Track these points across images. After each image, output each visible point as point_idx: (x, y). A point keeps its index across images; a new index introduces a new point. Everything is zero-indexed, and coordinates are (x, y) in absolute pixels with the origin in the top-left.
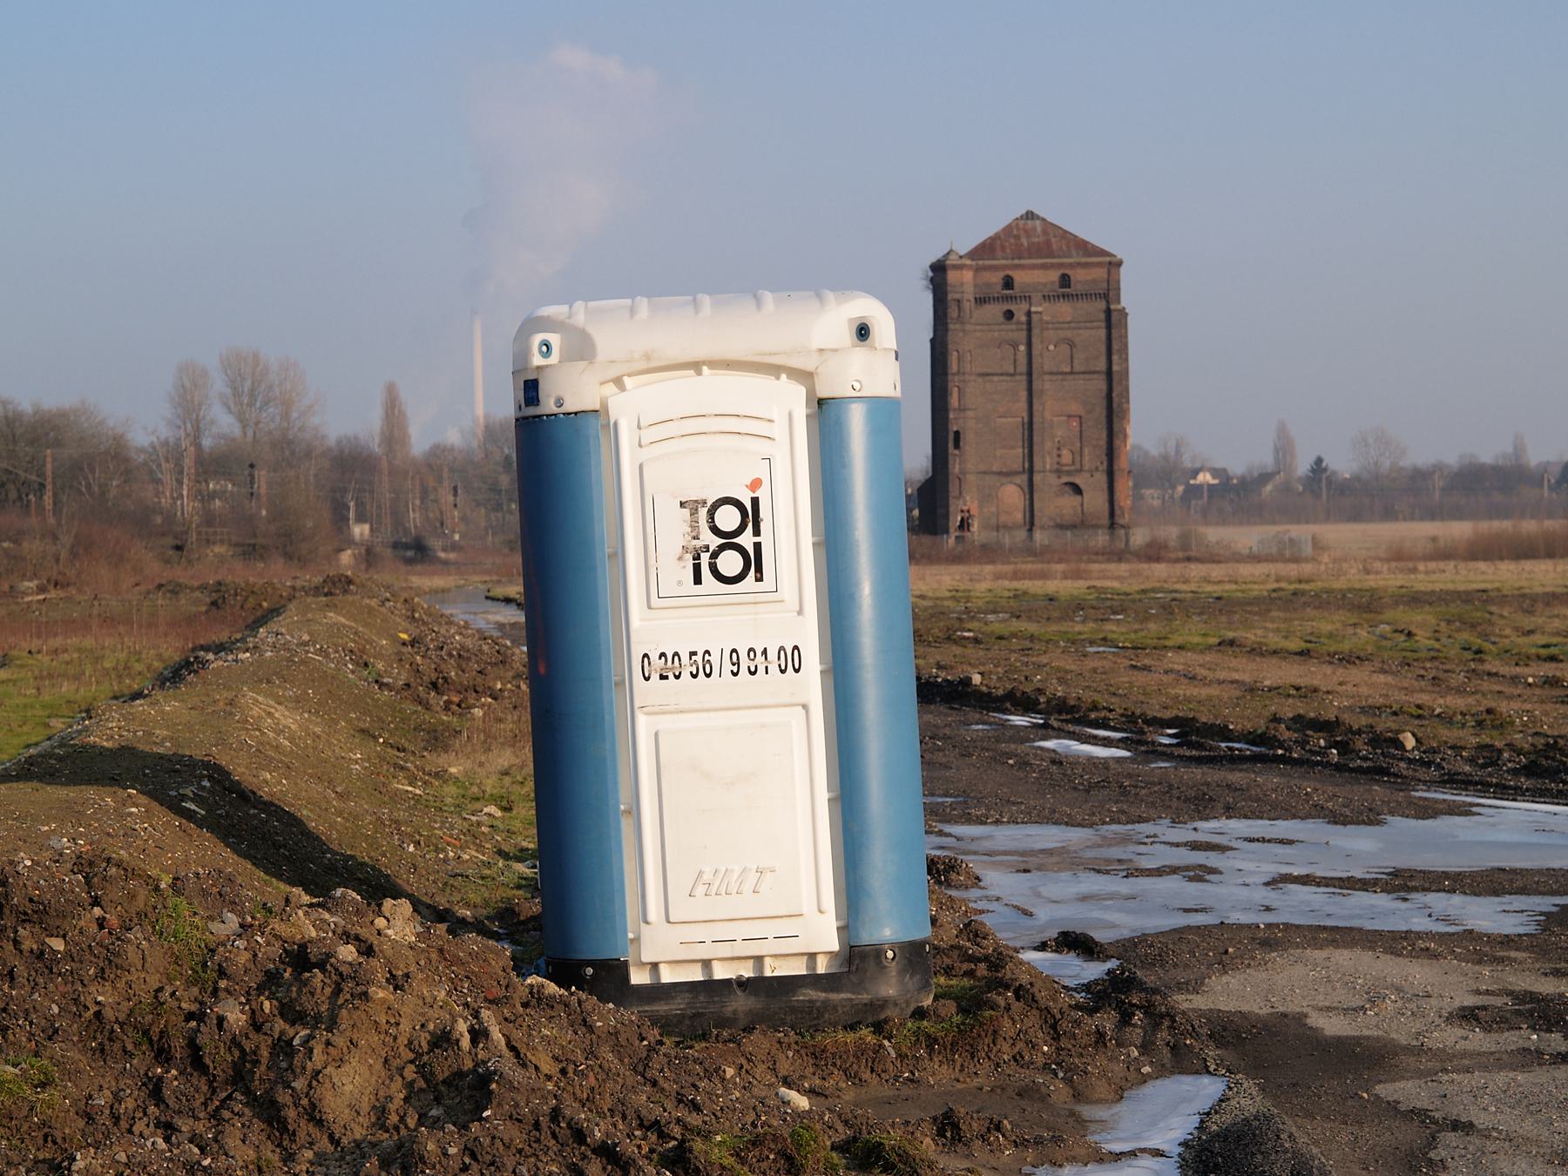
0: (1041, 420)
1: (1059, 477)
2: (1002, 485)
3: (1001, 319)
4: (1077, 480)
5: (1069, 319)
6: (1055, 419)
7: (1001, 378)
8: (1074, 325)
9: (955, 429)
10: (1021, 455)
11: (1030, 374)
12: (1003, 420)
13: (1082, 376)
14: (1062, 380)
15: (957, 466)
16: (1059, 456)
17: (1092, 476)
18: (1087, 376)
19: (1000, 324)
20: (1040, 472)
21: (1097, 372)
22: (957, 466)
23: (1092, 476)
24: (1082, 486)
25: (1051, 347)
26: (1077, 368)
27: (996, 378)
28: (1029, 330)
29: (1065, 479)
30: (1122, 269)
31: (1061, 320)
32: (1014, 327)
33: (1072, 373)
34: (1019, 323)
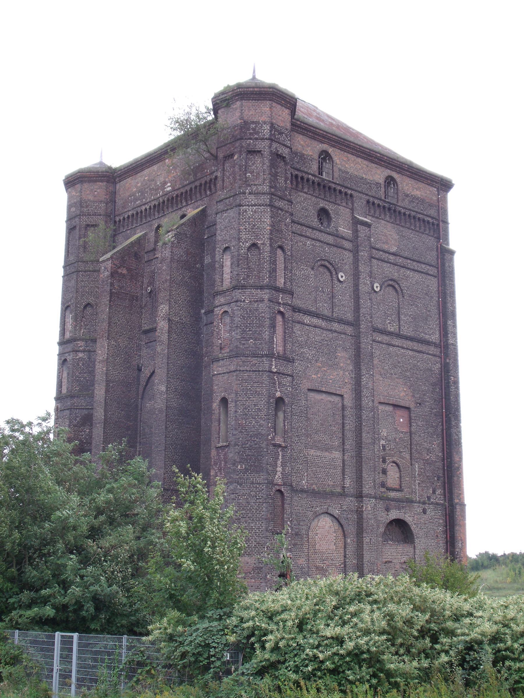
0: (370, 404)
1: (387, 510)
2: (317, 515)
3: (315, 223)
4: (408, 518)
5: (394, 249)
6: (381, 407)
7: (315, 321)
8: (400, 260)
9: (278, 394)
10: (339, 463)
11: (355, 324)
12: (319, 397)
13: (410, 344)
14: (389, 345)
15: (279, 469)
16: (384, 472)
17: (424, 511)
18: (416, 346)
19: (313, 229)
20: (369, 496)
21: (428, 343)
22: (279, 469)
23: (424, 511)
24: (413, 527)
25: (377, 287)
26: (407, 331)
27: (307, 319)
28: (355, 252)
29: (394, 515)
30: (451, 196)
31: (385, 247)
32: (330, 239)
33: (399, 336)
34: (337, 235)
